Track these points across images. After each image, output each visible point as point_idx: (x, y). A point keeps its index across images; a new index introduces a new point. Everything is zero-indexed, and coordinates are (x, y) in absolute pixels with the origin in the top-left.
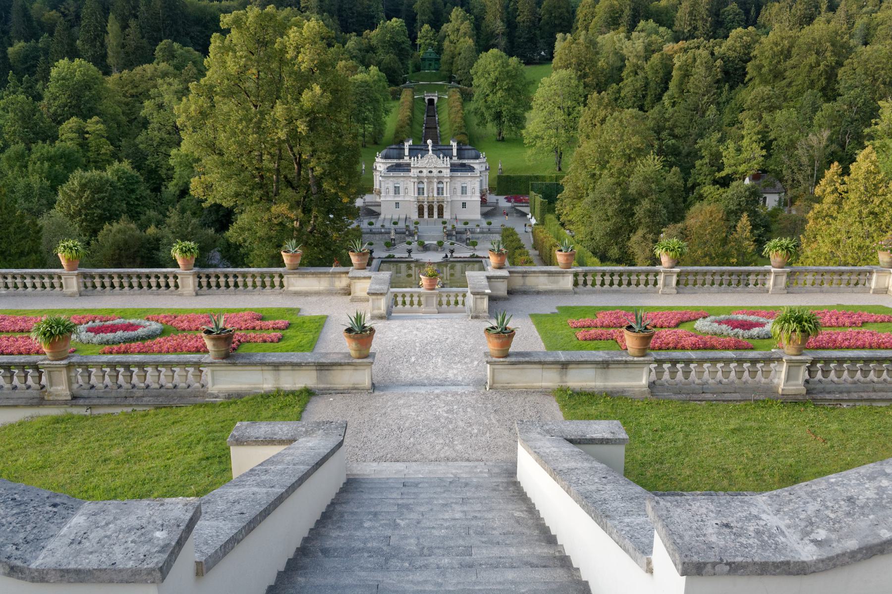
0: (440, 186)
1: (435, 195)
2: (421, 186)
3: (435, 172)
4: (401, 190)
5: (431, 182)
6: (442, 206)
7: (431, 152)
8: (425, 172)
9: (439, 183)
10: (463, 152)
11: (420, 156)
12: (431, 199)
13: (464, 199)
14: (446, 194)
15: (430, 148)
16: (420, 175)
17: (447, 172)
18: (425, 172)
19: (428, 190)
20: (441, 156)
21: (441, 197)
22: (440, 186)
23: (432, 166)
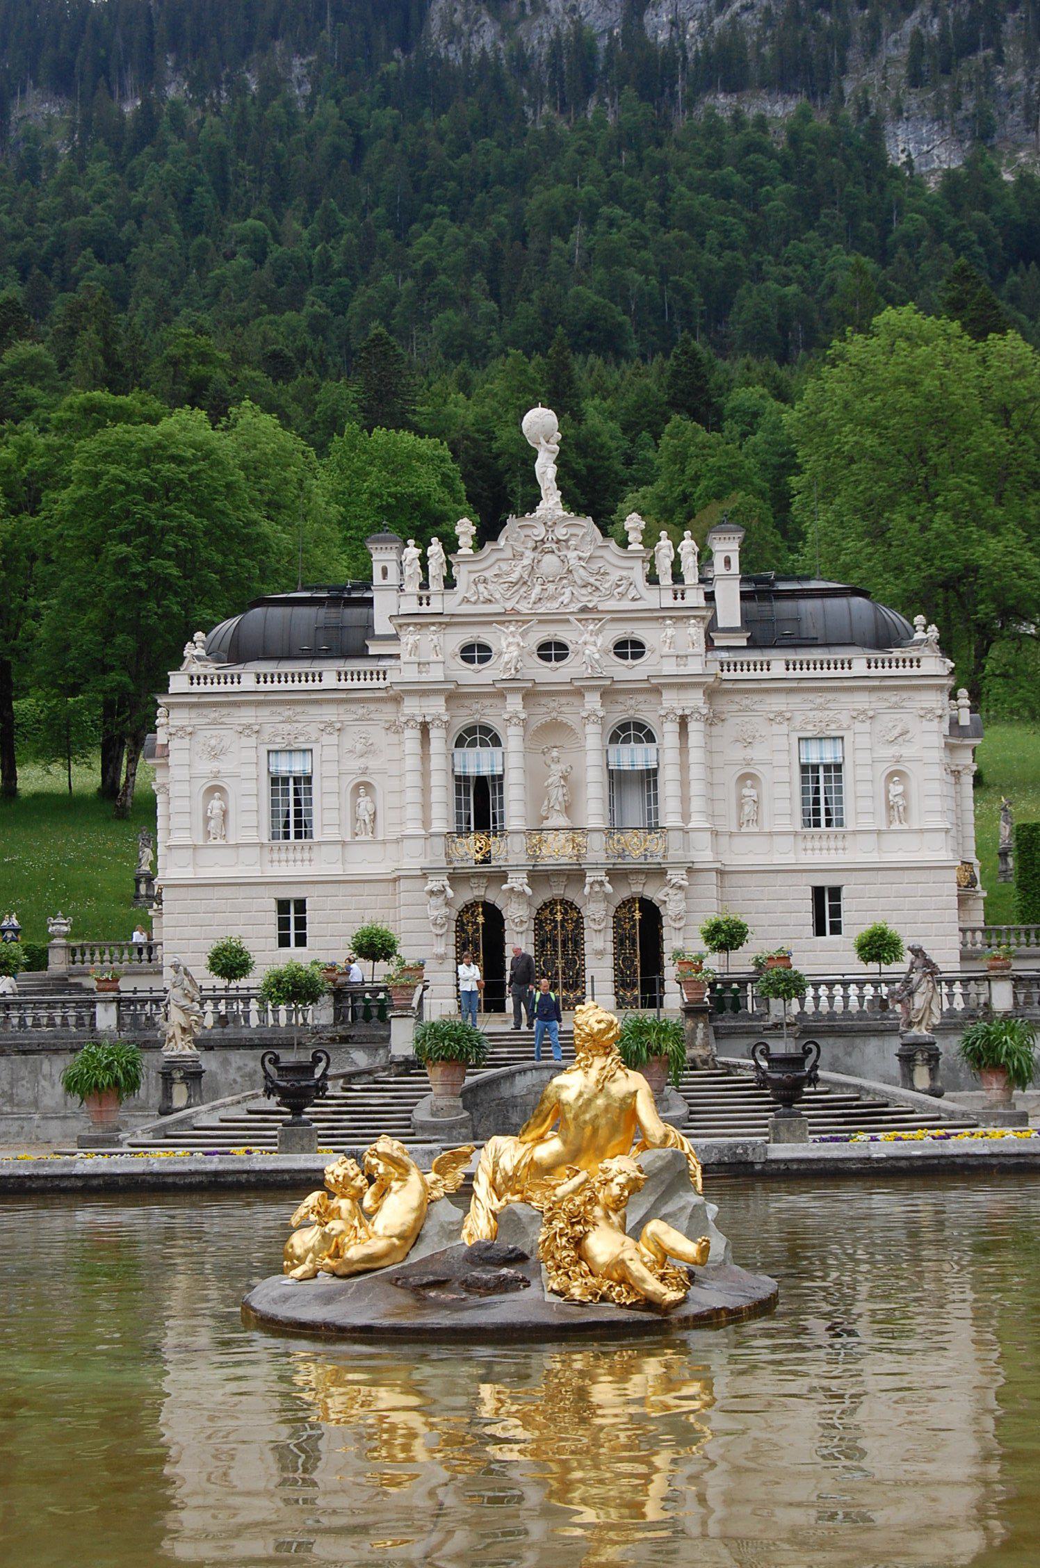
0: (633, 756)
1: (593, 812)
2: (479, 761)
3: (591, 648)
4: (326, 809)
5: (555, 727)
6: (651, 915)
7: (551, 501)
8: (512, 648)
9: (633, 731)
10: (785, 607)
11: (465, 529)
12: (557, 851)
13: (824, 855)
14: (691, 812)
15: (546, 469)
16: (470, 675)
17: (675, 649)
18: (512, 648)
19: (537, 795)
20: (634, 524)
21: (637, 847)
22: (633, 756)
23: (568, 599)
